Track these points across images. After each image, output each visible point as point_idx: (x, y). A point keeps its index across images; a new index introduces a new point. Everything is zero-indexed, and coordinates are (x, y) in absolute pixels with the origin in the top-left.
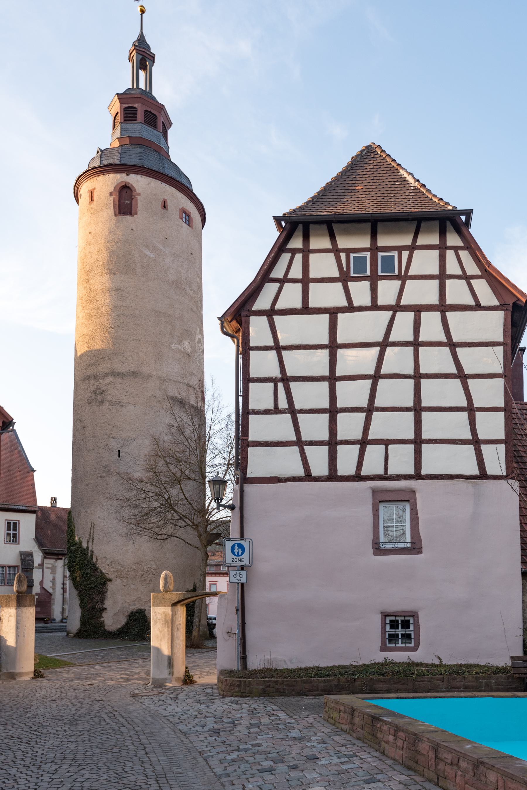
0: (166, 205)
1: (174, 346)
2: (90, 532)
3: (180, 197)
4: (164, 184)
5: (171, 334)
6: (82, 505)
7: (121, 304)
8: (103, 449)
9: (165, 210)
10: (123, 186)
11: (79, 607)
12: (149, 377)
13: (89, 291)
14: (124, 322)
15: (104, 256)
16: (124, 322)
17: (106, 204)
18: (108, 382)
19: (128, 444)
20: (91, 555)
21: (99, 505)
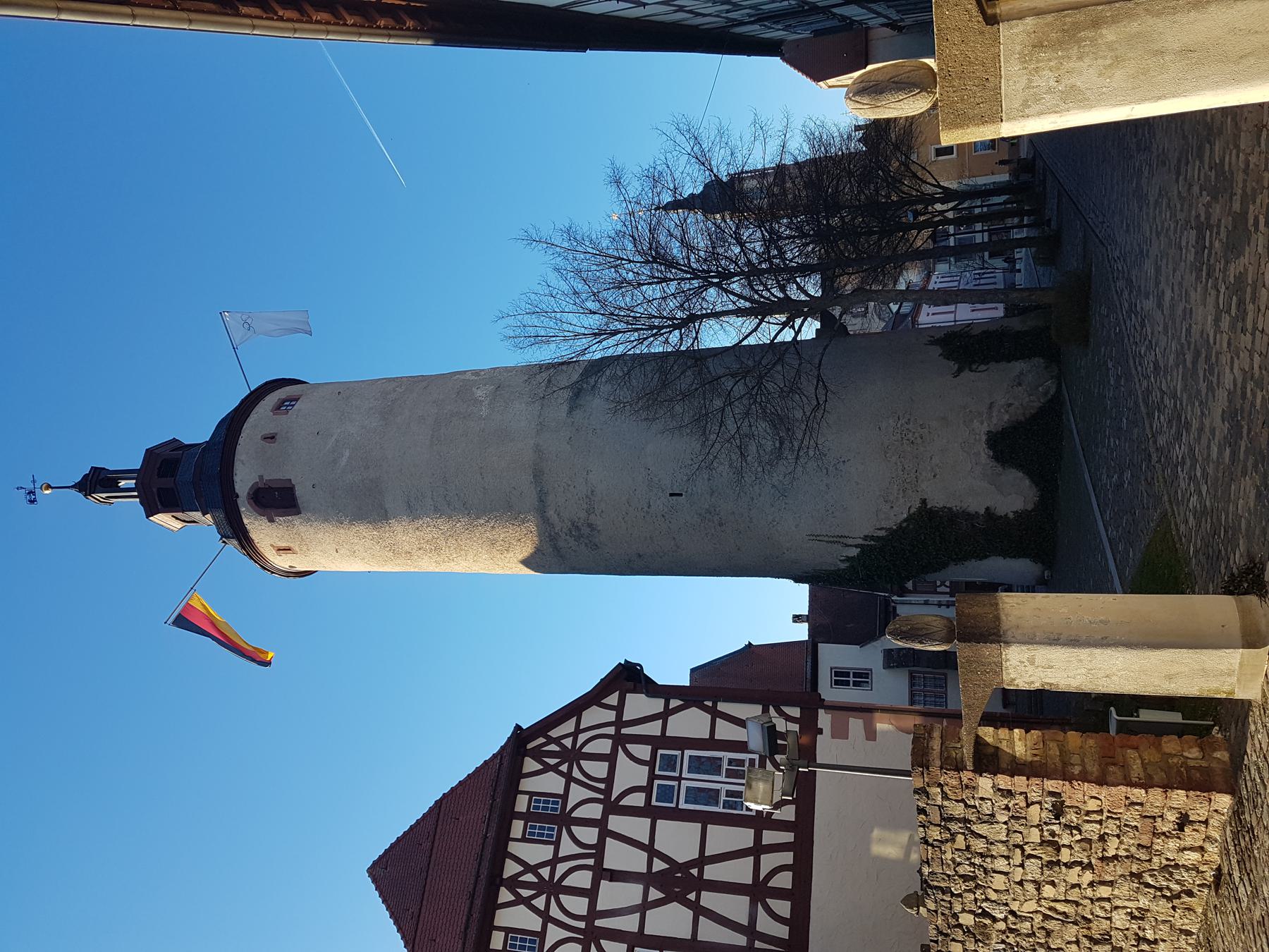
0: (269, 436)
1: (484, 412)
2: (827, 542)
3: (256, 415)
4: (241, 441)
5: (464, 417)
6: (777, 558)
7: (430, 500)
8: (670, 522)
9: (277, 437)
10: (255, 502)
11: (985, 562)
12: (538, 449)
13: (421, 552)
14: (457, 494)
15: (363, 529)
16: (457, 494)
17: (287, 527)
18: (556, 516)
19: (657, 479)
20: (873, 540)
21: (773, 526)
